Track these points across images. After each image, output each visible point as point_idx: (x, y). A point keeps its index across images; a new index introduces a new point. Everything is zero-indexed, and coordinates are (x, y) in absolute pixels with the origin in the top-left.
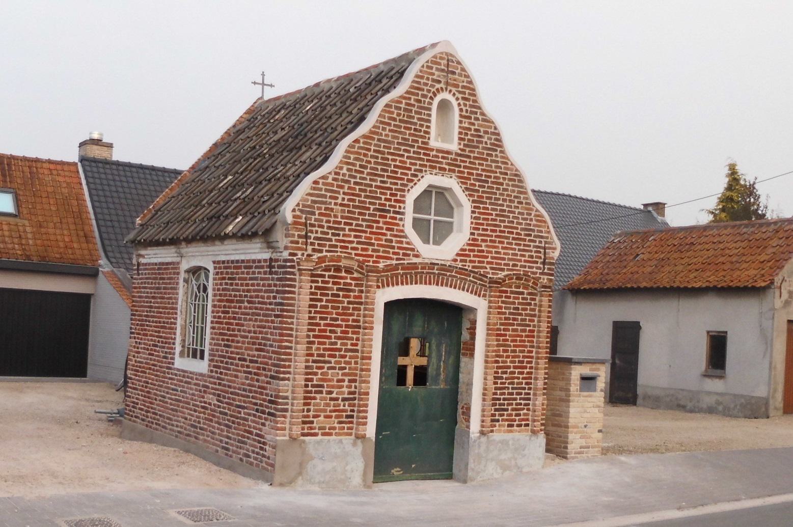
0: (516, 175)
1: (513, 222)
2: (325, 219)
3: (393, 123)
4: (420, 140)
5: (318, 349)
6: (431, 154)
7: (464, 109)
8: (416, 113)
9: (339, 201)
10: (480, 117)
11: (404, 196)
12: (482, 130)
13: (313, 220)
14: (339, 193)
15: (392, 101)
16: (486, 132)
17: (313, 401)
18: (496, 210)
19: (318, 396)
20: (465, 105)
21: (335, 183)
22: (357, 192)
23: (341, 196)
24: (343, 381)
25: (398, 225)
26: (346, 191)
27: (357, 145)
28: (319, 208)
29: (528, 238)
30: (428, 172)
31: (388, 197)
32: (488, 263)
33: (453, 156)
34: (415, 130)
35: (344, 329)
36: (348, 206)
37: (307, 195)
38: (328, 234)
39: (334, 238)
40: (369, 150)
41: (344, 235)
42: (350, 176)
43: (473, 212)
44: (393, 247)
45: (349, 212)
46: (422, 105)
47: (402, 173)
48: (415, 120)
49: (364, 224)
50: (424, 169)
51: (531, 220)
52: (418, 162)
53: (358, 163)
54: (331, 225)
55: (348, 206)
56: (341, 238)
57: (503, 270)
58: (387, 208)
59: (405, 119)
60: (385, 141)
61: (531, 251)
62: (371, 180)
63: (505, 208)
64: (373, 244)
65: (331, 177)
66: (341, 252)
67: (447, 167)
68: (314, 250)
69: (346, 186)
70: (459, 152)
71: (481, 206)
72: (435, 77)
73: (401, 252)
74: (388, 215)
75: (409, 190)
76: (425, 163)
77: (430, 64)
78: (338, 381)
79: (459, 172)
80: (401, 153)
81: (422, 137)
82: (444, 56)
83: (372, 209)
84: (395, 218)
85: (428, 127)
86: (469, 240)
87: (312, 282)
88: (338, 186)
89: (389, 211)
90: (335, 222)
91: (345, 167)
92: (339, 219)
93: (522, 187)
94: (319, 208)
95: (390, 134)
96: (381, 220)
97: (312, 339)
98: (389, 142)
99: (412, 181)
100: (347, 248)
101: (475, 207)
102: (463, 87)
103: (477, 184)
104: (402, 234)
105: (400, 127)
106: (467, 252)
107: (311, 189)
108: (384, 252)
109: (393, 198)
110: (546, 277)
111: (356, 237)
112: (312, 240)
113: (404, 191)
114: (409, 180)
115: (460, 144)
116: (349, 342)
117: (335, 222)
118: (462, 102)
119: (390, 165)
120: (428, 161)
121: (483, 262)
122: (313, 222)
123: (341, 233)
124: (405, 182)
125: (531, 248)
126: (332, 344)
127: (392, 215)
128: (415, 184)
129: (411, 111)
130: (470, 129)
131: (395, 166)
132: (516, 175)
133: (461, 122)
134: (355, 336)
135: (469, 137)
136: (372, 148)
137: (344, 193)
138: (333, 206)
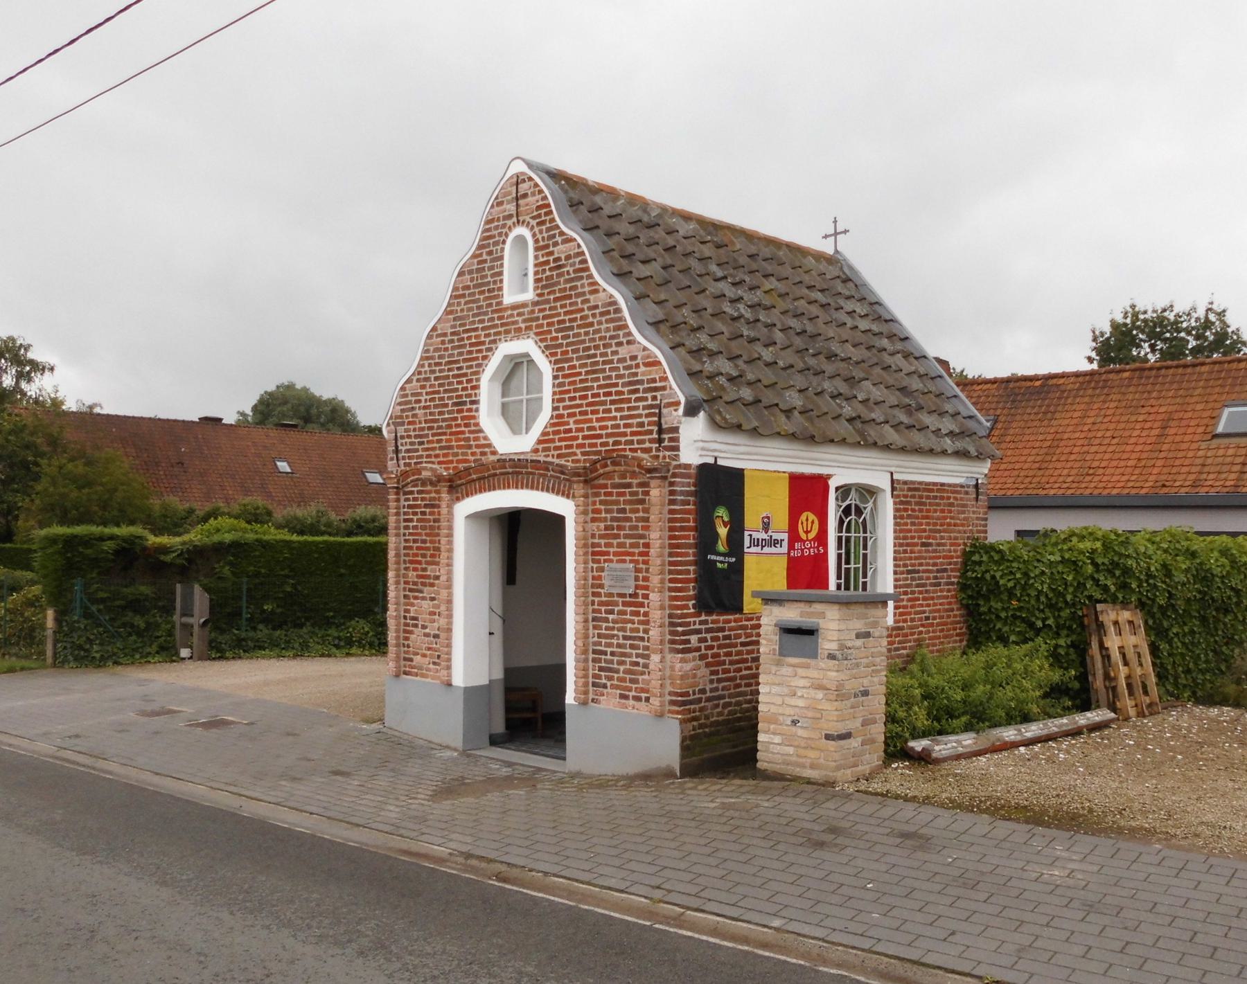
7: (539, 237)
9: (423, 404)
10: (559, 239)
25: (474, 417)
29: (633, 397)
32: (579, 446)
33: (529, 309)
43: (555, 377)
70: (537, 299)
79: (538, 326)
86: (552, 417)
91: (426, 363)
93: (620, 319)
115: (536, 288)
118: (536, 230)
125: (640, 411)
129: (483, 269)
133: (536, 257)
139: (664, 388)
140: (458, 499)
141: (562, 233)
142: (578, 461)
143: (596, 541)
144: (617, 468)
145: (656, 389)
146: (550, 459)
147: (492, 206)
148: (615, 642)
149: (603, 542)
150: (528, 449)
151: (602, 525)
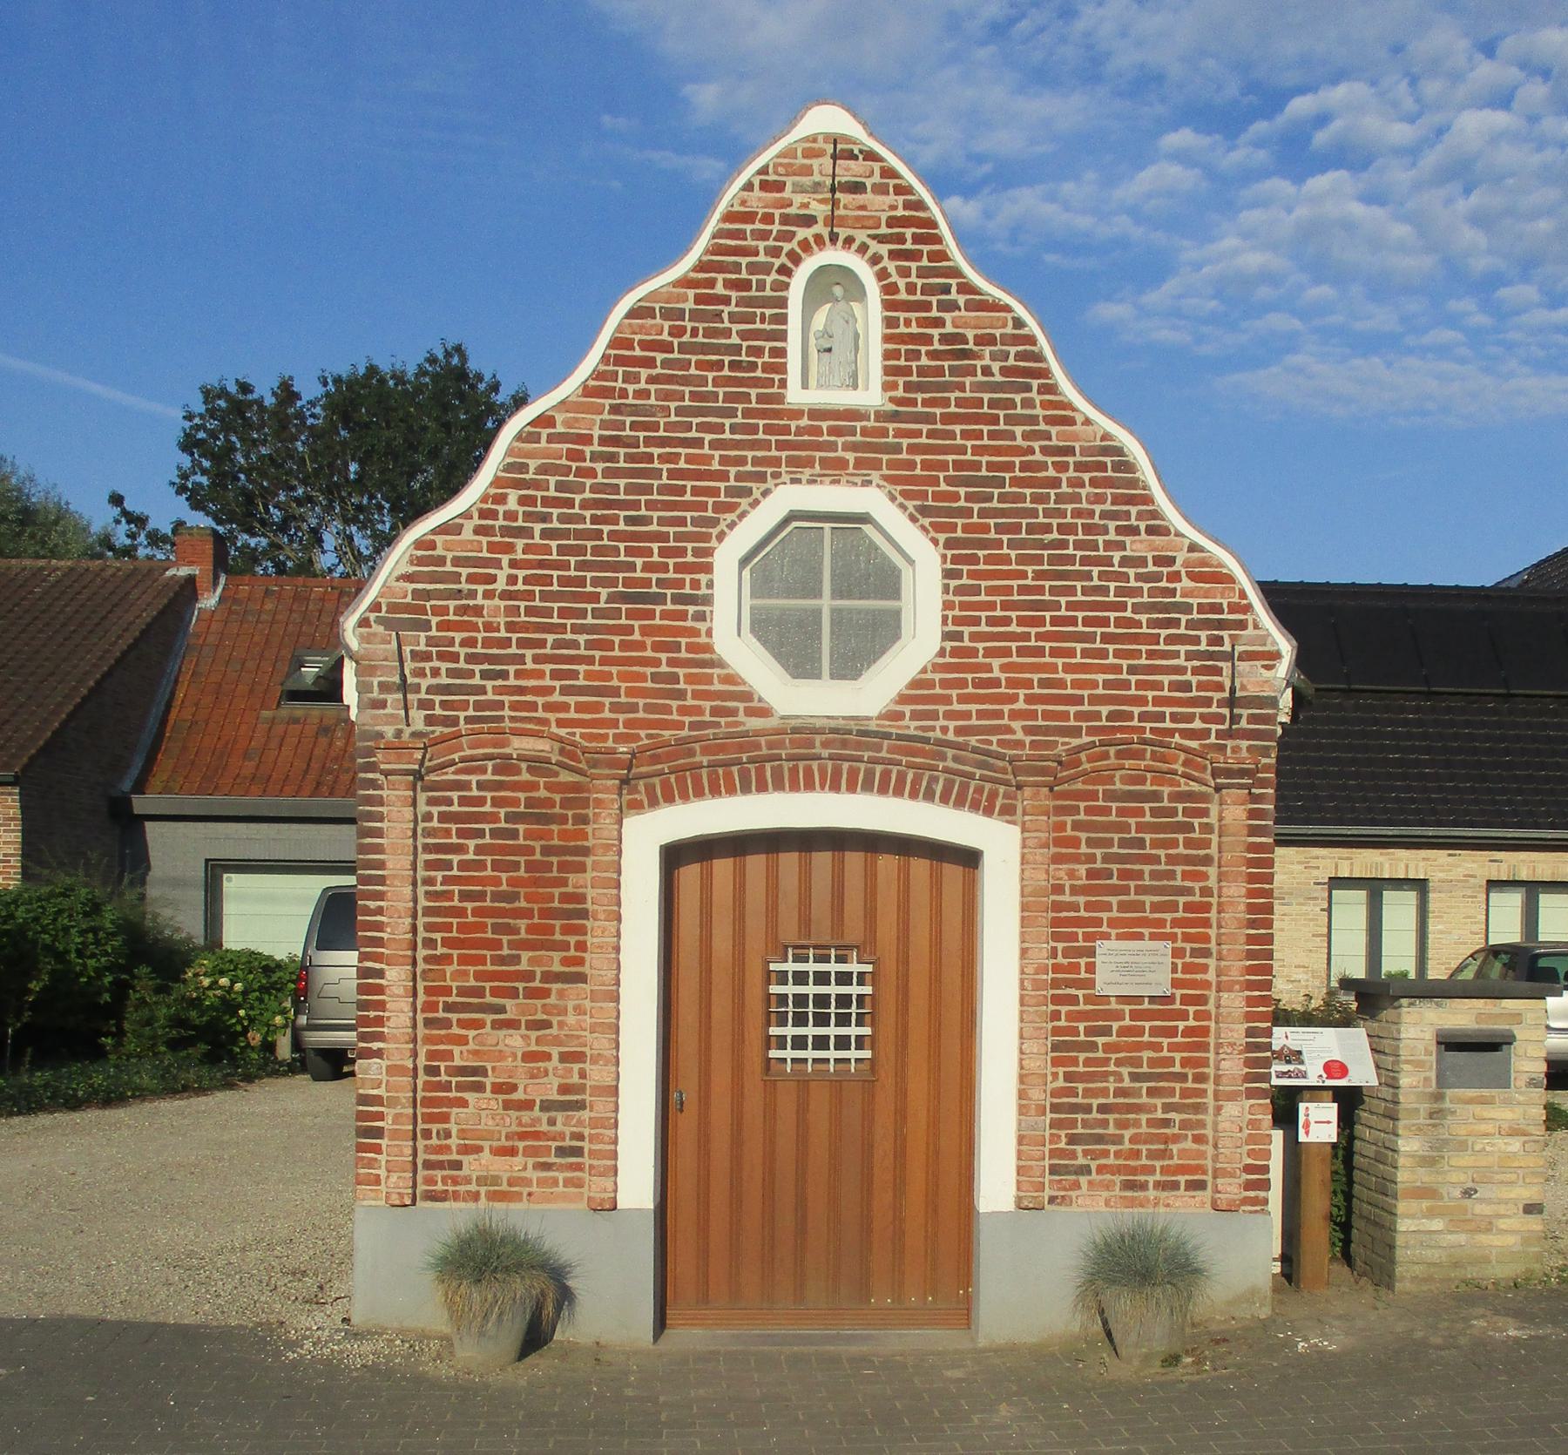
0: (1106, 451)
1: (1104, 591)
2: (458, 636)
3: (660, 357)
4: (753, 392)
5: (457, 975)
6: (793, 424)
7: (901, 283)
8: (734, 318)
9: (501, 585)
10: (961, 300)
11: (709, 552)
12: (970, 334)
13: (423, 641)
14: (497, 564)
15: (652, 296)
16: (981, 340)
17: (455, 1110)
18: (1038, 560)
19: (470, 1097)
20: (904, 273)
21: (484, 540)
22: (555, 557)
23: (502, 576)
24: (547, 1057)
26: (520, 556)
27: (545, 432)
28: (437, 611)
30: (786, 478)
31: (656, 558)
32: (1015, 715)
34: (734, 366)
35: (536, 920)
36: (530, 595)
37: (398, 580)
38: (471, 674)
39: (489, 684)
40: (587, 440)
41: (518, 674)
42: (528, 516)
43: (948, 574)
44: (681, 695)
45: (530, 611)
46: (753, 293)
47: (696, 491)
48: (735, 340)
49: (582, 638)
50: (769, 470)
51: (1175, 577)
52: (750, 454)
53: (552, 480)
54: (479, 650)
55: (530, 595)
56: (512, 682)
57: (1076, 732)
58: (654, 589)
59: (700, 339)
60: (635, 410)
61: (1180, 670)
62: (595, 520)
63: (1070, 551)
64: (615, 692)
65: (469, 526)
66: (512, 719)
67: (850, 457)
68: (430, 720)
69: (520, 543)
70: (892, 407)
71: (981, 553)
72: (792, 211)
73: (707, 705)
74: (658, 609)
75: (721, 537)
76: (774, 453)
77: (772, 177)
78: (529, 1057)
79: (892, 465)
80: (693, 434)
81: (756, 383)
82: (820, 144)
83: (603, 598)
84: (683, 616)
85: (782, 353)
86: (942, 653)
87: (431, 802)
88: (492, 547)
89: (660, 599)
90: (487, 643)
91: (513, 496)
92: (503, 634)
93: (1134, 483)
94: (444, 611)
95: (653, 388)
96: (636, 624)
97: (440, 951)
98: (649, 411)
99: (731, 508)
100: (533, 707)
101: (955, 559)
102: (892, 222)
103: (962, 491)
104: (707, 656)
105: (686, 365)
106: (938, 691)
107: (412, 563)
108: (648, 708)
109: (671, 562)
110: (1245, 744)
111: (555, 675)
112: (423, 696)
113: (706, 538)
114: (719, 508)
115: (888, 387)
116: (557, 956)
117: (487, 643)
118: (891, 266)
119: (657, 474)
120: (781, 446)
121: (998, 715)
122: (422, 647)
123: (512, 669)
124: (710, 514)
125: (1181, 662)
126: (501, 960)
127: (670, 606)
128: (742, 516)
129: (718, 316)
130: (927, 339)
131: (673, 474)
132: (1106, 451)
133: (890, 323)
134: (572, 939)
135: (924, 361)
136: (596, 433)
137: (514, 564)
138: (480, 601)
139: (1242, 625)
140: (636, 806)
141: (967, 288)
142: (1019, 744)
143: (1067, 898)
144: (1127, 763)
145: (1221, 625)
146: (938, 734)
147: (749, 187)
148: (1112, 1086)
149: (1082, 900)
150: (874, 713)
151: (1082, 869)
